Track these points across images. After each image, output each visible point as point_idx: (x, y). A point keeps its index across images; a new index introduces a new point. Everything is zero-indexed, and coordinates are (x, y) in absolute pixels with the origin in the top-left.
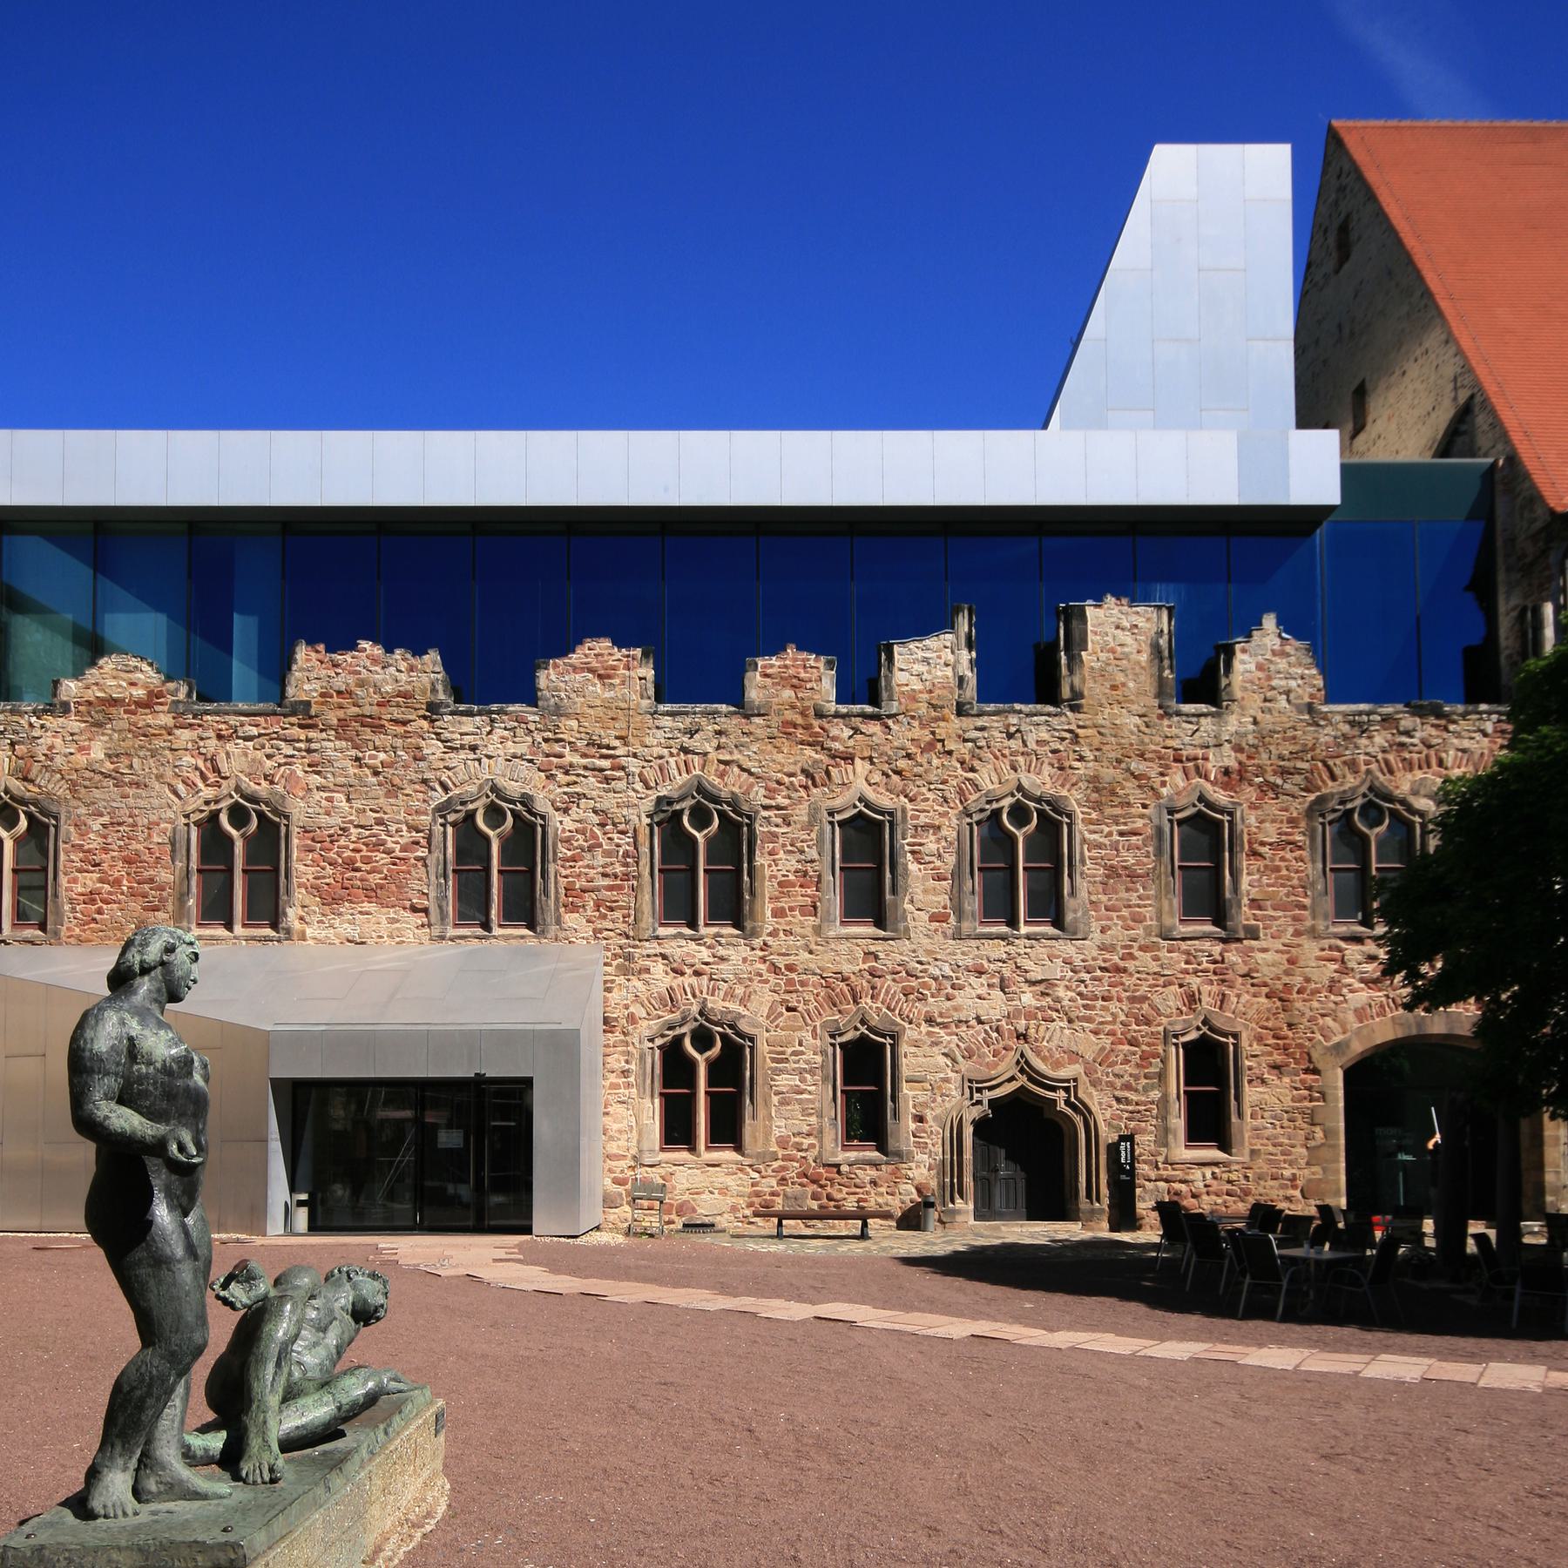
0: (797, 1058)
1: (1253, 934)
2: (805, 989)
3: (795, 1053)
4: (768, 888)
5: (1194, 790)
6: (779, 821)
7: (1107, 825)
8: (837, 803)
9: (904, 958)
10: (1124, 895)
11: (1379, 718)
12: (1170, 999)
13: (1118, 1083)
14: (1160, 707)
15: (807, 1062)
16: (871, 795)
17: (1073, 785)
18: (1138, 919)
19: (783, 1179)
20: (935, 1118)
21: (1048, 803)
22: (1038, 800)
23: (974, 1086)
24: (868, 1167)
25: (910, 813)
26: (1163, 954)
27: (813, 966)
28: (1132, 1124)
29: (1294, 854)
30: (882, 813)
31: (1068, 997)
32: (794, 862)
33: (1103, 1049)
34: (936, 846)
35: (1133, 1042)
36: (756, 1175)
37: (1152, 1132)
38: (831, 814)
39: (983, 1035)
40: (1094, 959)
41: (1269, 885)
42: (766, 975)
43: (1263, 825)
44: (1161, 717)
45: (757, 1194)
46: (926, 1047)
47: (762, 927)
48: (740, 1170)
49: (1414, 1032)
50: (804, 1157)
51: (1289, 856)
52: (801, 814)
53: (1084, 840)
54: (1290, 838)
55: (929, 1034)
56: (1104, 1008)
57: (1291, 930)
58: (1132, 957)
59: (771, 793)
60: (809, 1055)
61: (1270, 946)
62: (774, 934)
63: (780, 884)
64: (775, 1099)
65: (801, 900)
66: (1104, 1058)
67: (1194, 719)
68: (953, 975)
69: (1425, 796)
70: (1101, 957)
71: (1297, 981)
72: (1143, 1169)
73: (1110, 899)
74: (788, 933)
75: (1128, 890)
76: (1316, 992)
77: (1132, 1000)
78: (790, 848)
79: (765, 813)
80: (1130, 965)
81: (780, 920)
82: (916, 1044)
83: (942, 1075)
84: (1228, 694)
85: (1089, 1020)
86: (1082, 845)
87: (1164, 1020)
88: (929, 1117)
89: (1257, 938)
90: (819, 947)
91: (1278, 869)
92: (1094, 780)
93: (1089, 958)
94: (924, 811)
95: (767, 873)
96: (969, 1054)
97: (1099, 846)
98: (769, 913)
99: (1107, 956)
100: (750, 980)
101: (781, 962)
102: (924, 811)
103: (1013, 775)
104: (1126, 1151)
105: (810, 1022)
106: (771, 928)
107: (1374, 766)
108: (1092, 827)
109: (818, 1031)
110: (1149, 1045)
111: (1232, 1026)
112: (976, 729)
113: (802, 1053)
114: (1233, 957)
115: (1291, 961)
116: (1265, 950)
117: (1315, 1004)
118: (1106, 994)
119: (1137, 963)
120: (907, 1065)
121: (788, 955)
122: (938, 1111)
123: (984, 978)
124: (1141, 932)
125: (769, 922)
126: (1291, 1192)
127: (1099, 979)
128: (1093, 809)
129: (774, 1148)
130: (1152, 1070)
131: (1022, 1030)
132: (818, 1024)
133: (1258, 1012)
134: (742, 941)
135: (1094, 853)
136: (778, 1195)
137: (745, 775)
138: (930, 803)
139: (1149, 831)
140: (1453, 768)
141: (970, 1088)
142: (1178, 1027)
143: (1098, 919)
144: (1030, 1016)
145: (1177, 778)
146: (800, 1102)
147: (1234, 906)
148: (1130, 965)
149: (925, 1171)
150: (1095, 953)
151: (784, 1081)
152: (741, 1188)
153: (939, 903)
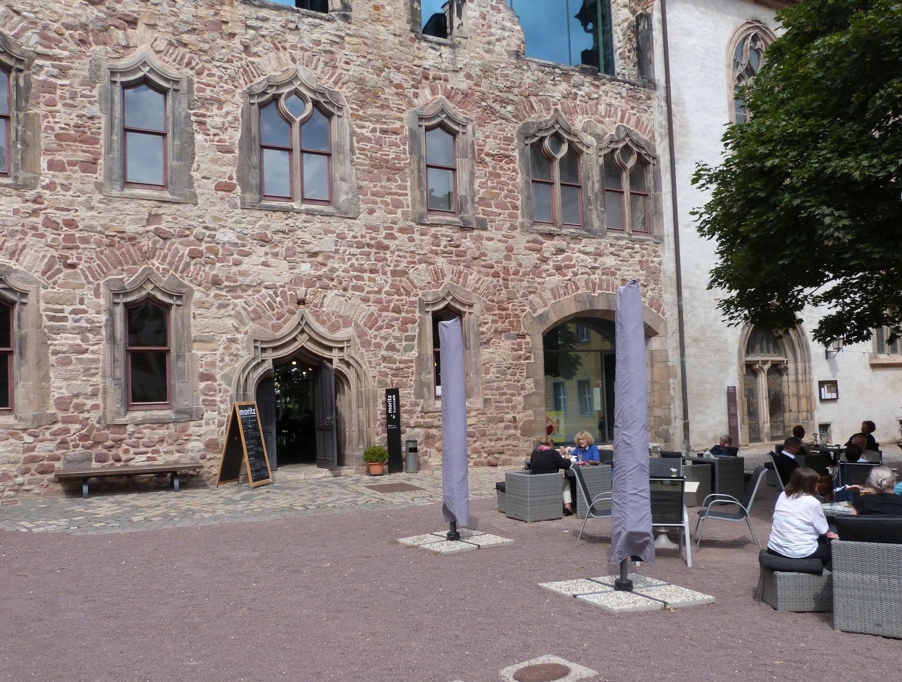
0: (78, 317)
2: (86, 246)
3: (74, 312)
4: (46, 140)
5: (438, 103)
6: (55, 71)
7: (370, 121)
8: (122, 63)
9: (192, 223)
10: (384, 183)
11: (560, 72)
12: (420, 275)
13: (385, 344)
14: (412, 31)
15: (88, 321)
16: (157, 62)
17: (343, 84)
18: (398, 205)
19: (64, 443)
20: (224, 377)
21: (322, 94)
22: (314, 92)
23: (261, 345)
24: (155, 426)
25: (196, 86)
26: (416, 236)
27: (95, 223)
28: (396, 380)
29: (509, 166)
30: (167, 80)
31: (342, 268)
32: (74, 116)
33: (372, 314)
34: (222, 120)
35: (397, 310)
36: (29, 439)
37: (411, 386)
38: (113, 73)
39: (268, 299)
40: (363, 236)
41: (493, 188)
42: (41, 229)
43: (487, 140)
44: (412, 40)
45: (32, 460)
46: (214, 309)
47: (36, 179)
48: (12, 435)
50: (88, 419)
51: (505, 167)
52: (81, 68)
53: (353, 133)
54: (507, 152)
55: (216, 296)
56: (371, 279)
57: (508, 225)
58: (393, 237)
59: (45, 39)
60: (91, 314)
61: (495, 236)
62: (50, 187)
63: (58, 136)
64: (53, 359)
65: (81, 156)
66: (372, 322)
67: (437, 47)
68: (240, 242)
69: (590, 134)
70: (368, 235)
72: (404, 417)
73: (375, 186)
74: (66, 188)
75: (389, 180)
77: (394, 273)
78: (69, 101)
79: (39, 62)
80: (392, 244)
81: (57, 173)
82: (201, 304)
83: (229, 336)
84: (461, 32)
85: (360, 289)
86: (351, 137)
87: (420, 292)
88: (218, 377)
89: (485, 229)
90: (102, 205)
91: (499, 176)
92: (361, 81)
93: (359, 235)
94: (209, 85)
95: (44, 124)
96: (257, 316)
97: (369, 140)
98: (44, 164)
99: (373, 235)
100: (25, 234)
101: (59, 217)
102: (209, 85)
103: (292, 66)
104: (392, 402)
105: (91, 279)
106: (47, 181)
107: (559, 107)
108: (358, 122)
109: (102, 290)
111: (469, 299)
112: (257, 19)
113: (86, 312)
114: (467, 242)
115: (510, 249)
116: (490, 239)
117: (525, 284)
118: (373, 267)
119: (397, 242)
120: (195, 326)
121: (69, 210)
122: (226, 370)
123: (267, 249)
124: (399, 215)
125: (46, 177)
126: (512, 431)
127: (368, 254)
128: (361, 107)
129: (53, 410)
130: (410, 333)
131: (301, 295)
132: (102, 282)
133: (488, 288)
134: (14, 192)
136: (58, 459)
137: (16, 18)
138: (216, 78)
139: (406, 132)
140: (605, 117)
141: (256, 347)
142: (430, 298)
144: (310, 284)
145: (426, 93)
146: (80, 361)
147: (469, 201)
148: (392, 244)
149: (212, 427)
150: (364, 231)
151: (63, 341)
152: (13, 454)
153: (225, 173)
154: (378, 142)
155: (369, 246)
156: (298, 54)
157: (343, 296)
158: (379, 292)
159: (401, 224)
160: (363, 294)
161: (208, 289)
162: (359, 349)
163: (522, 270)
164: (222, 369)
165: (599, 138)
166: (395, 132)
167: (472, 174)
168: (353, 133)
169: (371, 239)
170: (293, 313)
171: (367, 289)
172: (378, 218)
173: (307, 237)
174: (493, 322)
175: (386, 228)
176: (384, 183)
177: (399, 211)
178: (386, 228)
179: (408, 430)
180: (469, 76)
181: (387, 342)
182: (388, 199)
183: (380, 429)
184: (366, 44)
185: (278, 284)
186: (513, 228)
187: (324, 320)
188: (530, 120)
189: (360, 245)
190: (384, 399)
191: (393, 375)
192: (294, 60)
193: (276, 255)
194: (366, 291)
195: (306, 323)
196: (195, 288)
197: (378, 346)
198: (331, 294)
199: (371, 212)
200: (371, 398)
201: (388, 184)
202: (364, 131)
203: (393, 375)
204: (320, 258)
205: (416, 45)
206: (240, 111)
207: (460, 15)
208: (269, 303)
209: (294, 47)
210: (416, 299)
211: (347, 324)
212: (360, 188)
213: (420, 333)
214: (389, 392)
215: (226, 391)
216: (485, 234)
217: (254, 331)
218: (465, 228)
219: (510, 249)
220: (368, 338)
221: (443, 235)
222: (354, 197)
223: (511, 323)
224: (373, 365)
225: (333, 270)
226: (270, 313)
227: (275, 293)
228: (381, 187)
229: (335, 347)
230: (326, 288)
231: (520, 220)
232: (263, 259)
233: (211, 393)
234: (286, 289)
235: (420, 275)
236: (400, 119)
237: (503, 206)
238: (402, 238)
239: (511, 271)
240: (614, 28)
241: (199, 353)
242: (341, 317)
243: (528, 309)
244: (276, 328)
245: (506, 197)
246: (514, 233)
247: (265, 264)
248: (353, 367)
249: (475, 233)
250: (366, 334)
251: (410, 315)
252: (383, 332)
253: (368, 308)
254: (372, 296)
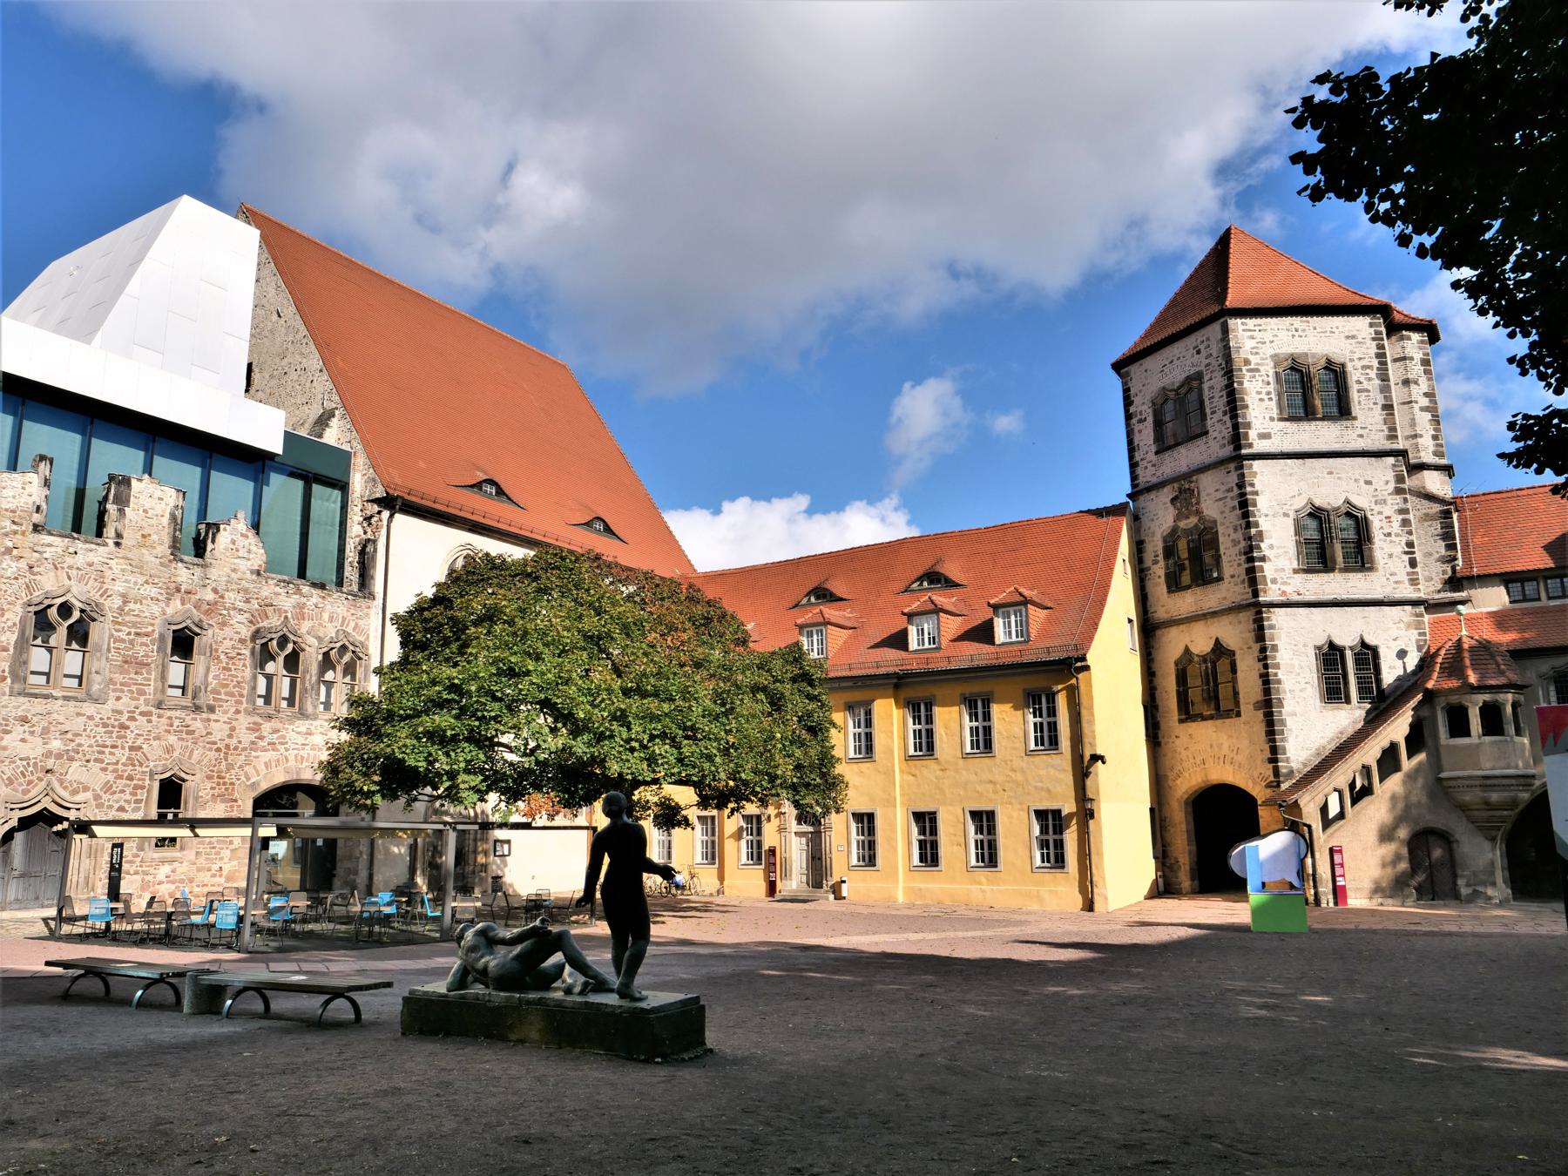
1: (212, 709)
5: (186, 612)
10: (132, 676)
13: (116, 806)
18: (141, 693)
26: (154, 718)
33: (109, 781)
35: (130, 778)
39: (22, 769)
40: (108, 718)
41: (224, 679)
49: (295, 777)
53: (111, 636)
56: (111, 753)
57: (233, 710)
58: (132, 719)
66: (108, 788)
67: (191, 567)
71: (233, 742)
72: (125, 866)
75: (136, 673)
76: (244, 749)
77: (131, 748)
80: (132, 724)
85: (102, 761)
86: (110, 638)
91: (230, 670)
97: (123, 641)
99: (118, 717)
103: (67, 582)
108: (117, 627)
110: (139, 780)
115: (233, 729)
117: (243, 758)
119: (137, 723)
124: (142, 701)
130: (139, 797)
133: (210, 760)
135: (116, 645)
139: (156, 635)
143: (114, 691)
144: (59, 756)
148: (132, 724)
154: (131, 642)
155: (113, 727)
156: (73, 573)
158: (117, 763)
159: (143, 708)
160: (103, 765)
163: (241, 746)
165: (320, 639)
166: (147, 635)
167: (208, 670)
168: (111, 636)
169: (116, 720)
170: (42, 780)
171: (106, 761)
172: (123, 704)
173: (61, 719)
174: (212, 788)
175: (128, 712)
176: (132, 676)
177: (142, 698)
178: (128, 712)
179: (127, 876)
180: (215, 591)
181: (118, 805)
182: (134, 688)
183: (103, 876)
184: (131, 565)
186: (238, 712)
188: (261, 625)
189: (105, 725)
190: (110, 851)
192: (70, 578)
193: (32, 733)
195: (52, 789)
197: (110, 807)
198: (75, 764)
199: (118, 699)
200: (99, 849)
201: (135, 677)
202: (120, 634)
204: (69, 736)
205: (174, 565)
206: (19, 618)
207: (213, 542)
208: (22, 773)
209: (70, 567)
210: (148, 769)
211: (86, 789)
212: (111, 679)
213: (147, 797)
214: (115, 846)
216: (213, 717)
217: (6, 796)
218: (197, 709)
219: (233, 729)
221: (176, 718)
222: (105, 687)
223: (226, 789)
225: (80, 745)
226: (22, 780)
227: (28, 764)
228: (130, 679)
230: (71, 759)
231: (245, 705)
232: (21, 736)
235: (154, 750)
236: (153, 625)
237: (232, 695)
238: (142, 720)
239: (232, 748)
240: (348, 540)
243: (243, 778)
244: (25, 792)
245: (234, 687)
246: (238, 716)
247: (23, 740)
249: (204, 716)
250: (101, 798)
251: (140, 783)
252: (116, 796)
254: (110, 768)
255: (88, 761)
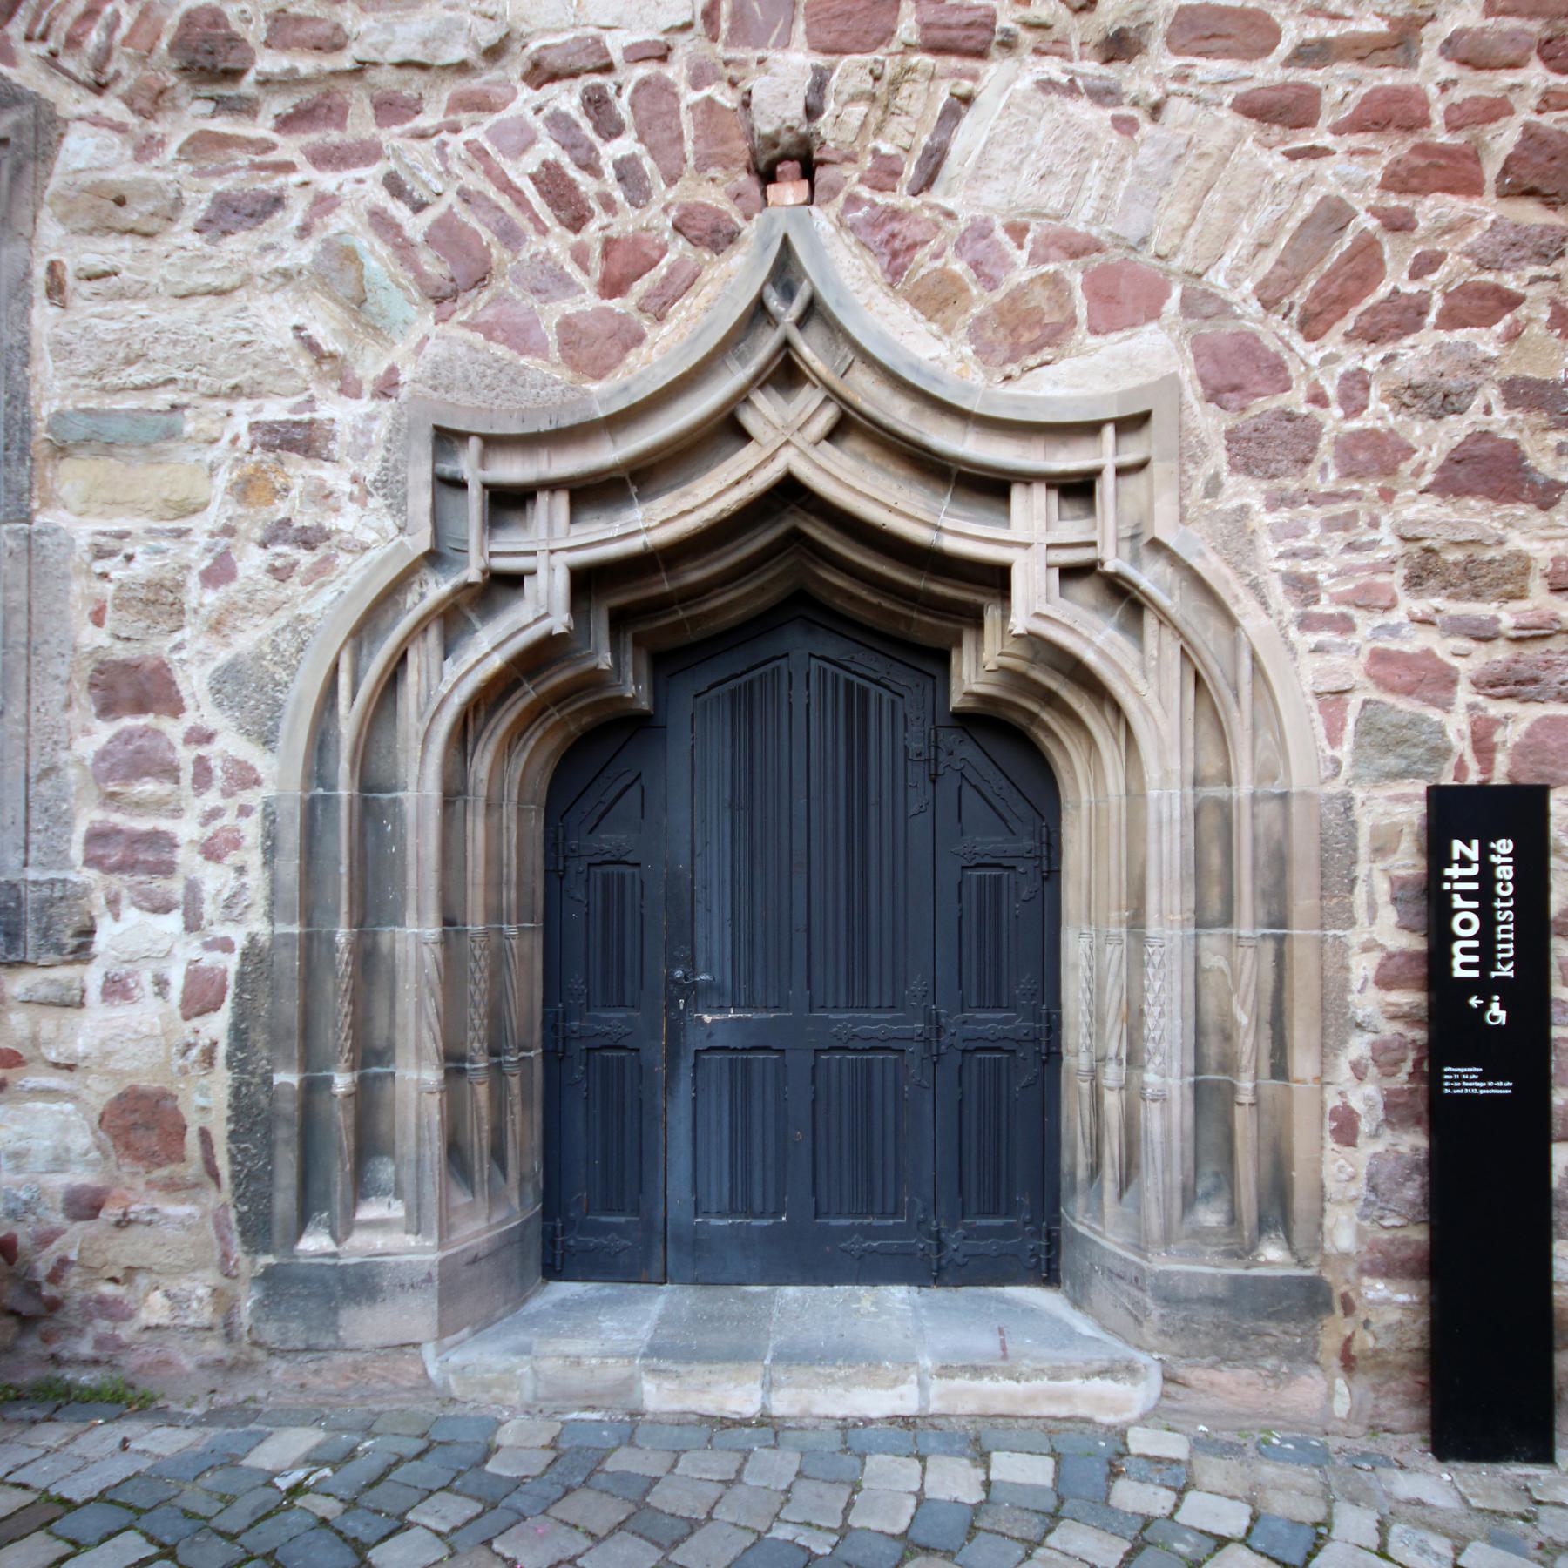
33: (1334, 215)
39: (548, 149)
46: (182, 235)
55: (202, 145)
83: (276, 410)
88: (193, 681)
104: (1485, 895)
120: (62, 349)
122: (248, 638)
141: (452, 484)
157: (1103, 95)
160: (1267, 72)
161: (152, 102)
162: (1213, 487)
164: (217, 627)
170: (719, 237)
171: (1293, 32)
181: (1456, 429)
183: (1365, 1098)
185: (615, 45)
187: (947, 278)
190: (1408, 861)
191: (1497, 684)
194: (1284, 48)
195: (813, 311)
196: (70, 101)
200: (1304, 851)
203: (1497, 684)
215: (244, 777)
217: (437, 377)
220: (1296, 400)
224: (1325, 607)
226: (557, 243)
229: (1028, 478)
233: (148, 788)
234: (675, 72)
241: (84, 531)
242: (1078, 249)
248: (1164, 619)
250: (1276, 373)
253: (1299, 171)
255: (1119, 47)
